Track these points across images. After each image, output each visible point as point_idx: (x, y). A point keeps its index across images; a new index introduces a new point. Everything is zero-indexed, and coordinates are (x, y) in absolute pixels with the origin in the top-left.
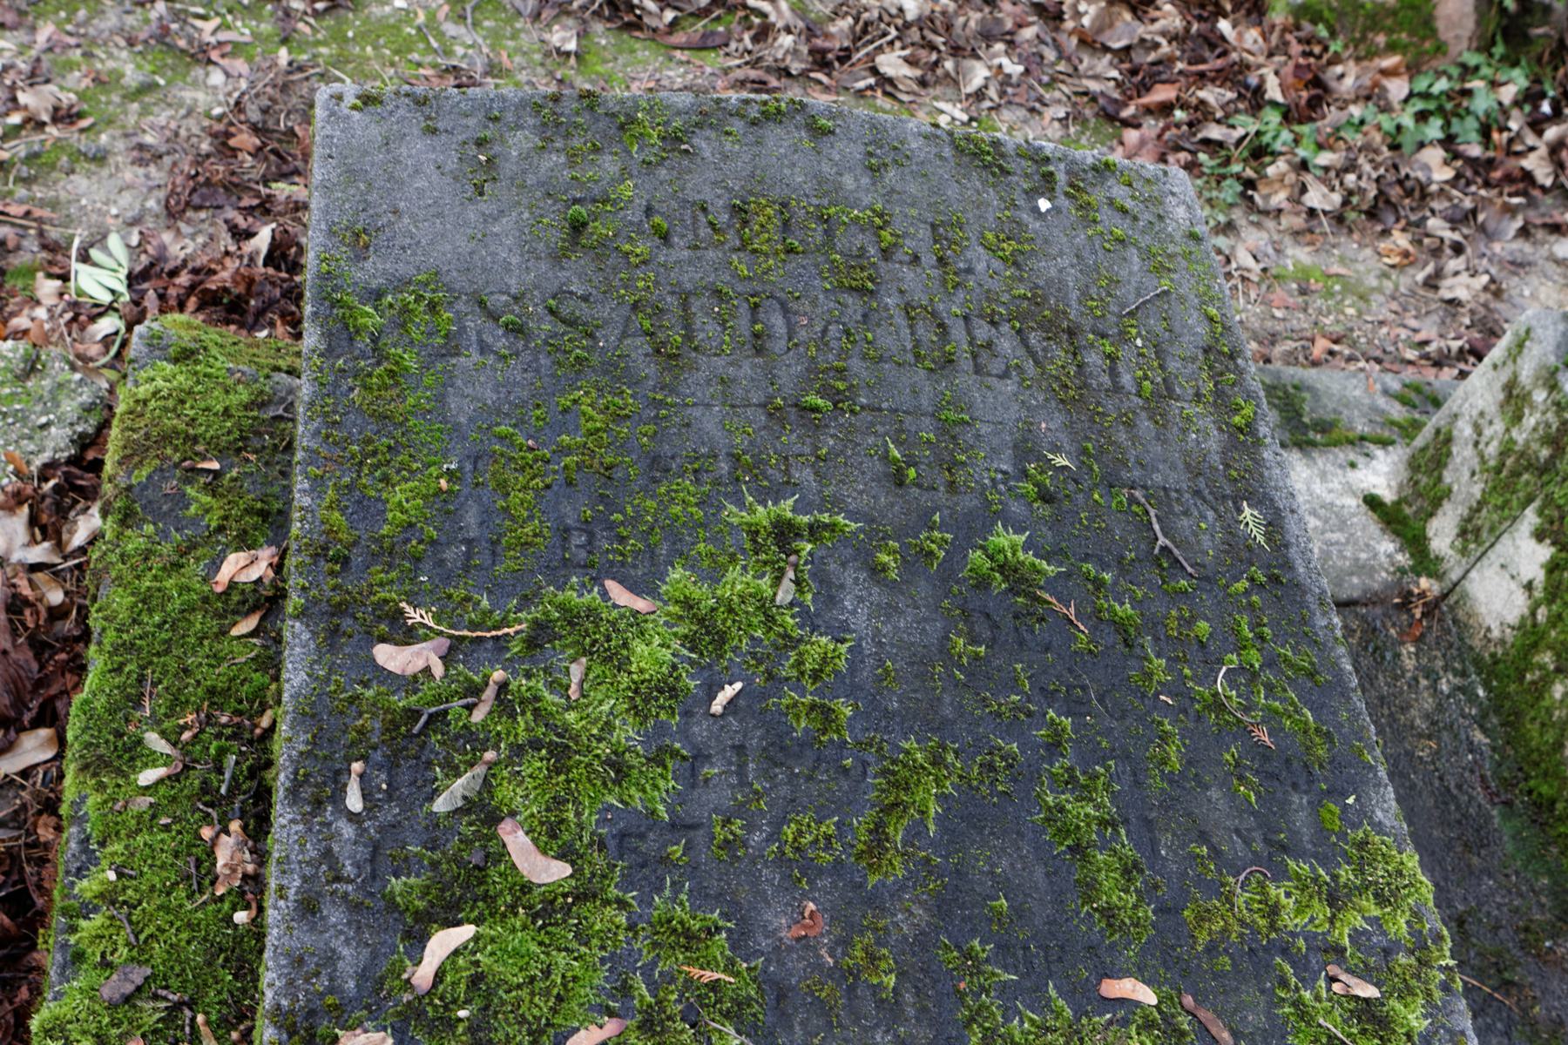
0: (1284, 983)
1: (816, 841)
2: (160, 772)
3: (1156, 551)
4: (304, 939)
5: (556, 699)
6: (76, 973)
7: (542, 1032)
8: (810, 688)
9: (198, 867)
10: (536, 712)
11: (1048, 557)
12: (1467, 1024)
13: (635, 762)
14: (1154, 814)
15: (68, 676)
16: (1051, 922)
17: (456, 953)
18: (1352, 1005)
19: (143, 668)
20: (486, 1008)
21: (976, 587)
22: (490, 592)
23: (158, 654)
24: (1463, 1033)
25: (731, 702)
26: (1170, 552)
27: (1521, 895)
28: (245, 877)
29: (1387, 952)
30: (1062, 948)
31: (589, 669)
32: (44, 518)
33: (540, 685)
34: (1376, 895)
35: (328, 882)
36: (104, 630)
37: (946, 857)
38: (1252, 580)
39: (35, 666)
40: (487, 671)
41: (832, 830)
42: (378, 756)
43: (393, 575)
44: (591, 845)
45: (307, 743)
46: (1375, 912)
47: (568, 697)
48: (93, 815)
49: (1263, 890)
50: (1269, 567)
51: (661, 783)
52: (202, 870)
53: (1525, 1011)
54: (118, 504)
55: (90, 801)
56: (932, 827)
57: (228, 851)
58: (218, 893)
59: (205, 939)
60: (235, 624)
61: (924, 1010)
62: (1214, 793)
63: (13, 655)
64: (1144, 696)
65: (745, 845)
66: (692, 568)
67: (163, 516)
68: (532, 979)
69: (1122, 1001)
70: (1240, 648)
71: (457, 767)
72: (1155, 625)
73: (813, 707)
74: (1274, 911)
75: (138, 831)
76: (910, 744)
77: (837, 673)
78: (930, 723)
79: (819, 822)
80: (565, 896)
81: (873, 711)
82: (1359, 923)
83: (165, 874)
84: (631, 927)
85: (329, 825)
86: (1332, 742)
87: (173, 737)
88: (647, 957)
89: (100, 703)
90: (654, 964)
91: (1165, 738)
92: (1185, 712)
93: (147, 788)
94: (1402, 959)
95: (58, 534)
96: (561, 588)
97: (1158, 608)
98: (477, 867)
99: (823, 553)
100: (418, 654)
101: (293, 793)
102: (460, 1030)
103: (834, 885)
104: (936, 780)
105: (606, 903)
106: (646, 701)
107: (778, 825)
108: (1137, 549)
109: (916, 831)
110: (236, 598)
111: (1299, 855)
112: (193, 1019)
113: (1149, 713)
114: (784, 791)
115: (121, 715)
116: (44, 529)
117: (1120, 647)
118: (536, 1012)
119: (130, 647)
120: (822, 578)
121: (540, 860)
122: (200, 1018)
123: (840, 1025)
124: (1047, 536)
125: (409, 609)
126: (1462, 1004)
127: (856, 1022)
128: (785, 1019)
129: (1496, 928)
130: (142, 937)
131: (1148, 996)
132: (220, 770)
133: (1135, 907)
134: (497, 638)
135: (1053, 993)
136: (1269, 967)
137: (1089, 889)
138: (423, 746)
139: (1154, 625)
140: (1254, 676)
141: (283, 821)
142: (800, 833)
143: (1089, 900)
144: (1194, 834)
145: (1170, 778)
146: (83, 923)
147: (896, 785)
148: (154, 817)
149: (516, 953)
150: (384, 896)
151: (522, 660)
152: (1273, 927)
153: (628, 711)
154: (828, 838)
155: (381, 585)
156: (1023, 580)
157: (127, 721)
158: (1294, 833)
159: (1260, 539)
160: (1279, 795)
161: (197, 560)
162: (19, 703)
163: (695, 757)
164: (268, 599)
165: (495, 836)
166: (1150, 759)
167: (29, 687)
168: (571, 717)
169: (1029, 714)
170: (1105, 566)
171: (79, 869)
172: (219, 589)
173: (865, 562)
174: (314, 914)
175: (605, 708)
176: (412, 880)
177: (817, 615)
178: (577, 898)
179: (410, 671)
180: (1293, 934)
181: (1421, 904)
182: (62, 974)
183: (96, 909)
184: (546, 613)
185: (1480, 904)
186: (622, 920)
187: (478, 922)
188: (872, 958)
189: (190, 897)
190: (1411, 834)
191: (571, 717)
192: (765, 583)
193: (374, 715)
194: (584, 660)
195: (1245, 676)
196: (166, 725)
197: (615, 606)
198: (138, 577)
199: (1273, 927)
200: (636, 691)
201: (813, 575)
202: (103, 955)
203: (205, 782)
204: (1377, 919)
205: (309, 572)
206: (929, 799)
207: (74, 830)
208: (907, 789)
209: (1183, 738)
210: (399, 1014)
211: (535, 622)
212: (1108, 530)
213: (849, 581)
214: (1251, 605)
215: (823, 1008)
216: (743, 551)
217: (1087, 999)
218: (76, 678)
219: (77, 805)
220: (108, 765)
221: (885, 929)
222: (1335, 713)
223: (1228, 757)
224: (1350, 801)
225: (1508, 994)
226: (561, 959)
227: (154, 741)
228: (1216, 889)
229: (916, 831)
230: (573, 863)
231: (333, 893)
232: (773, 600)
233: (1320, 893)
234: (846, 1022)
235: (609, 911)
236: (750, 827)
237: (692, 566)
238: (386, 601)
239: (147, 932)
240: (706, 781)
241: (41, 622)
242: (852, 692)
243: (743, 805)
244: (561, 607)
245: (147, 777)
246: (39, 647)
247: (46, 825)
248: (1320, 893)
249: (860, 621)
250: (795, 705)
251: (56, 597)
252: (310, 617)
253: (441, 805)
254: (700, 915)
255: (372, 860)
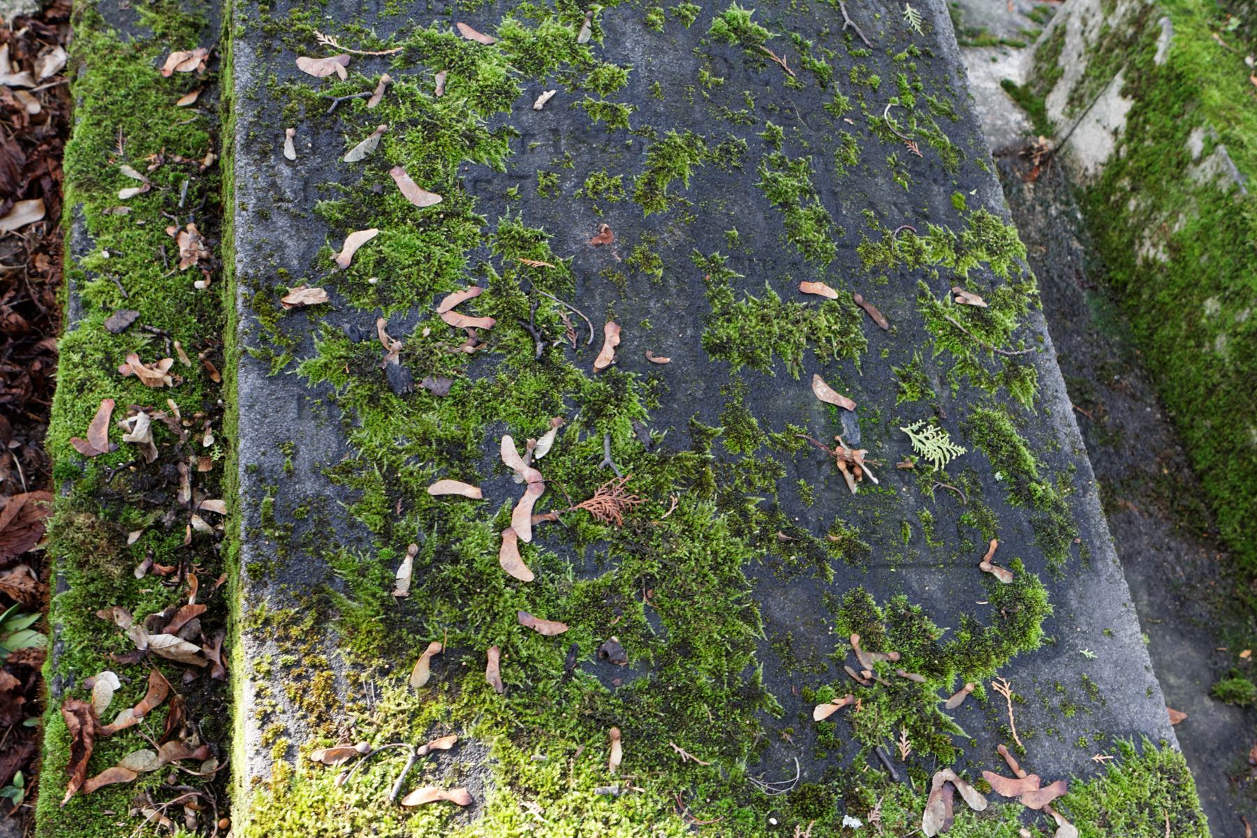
0: (923, 295)
1: (608, 188)
2: (134, 191)
3: (844, 28)
4: (260, 234)
5: (427, 96)
6: (87, 313)
7: (426, 294)
8: (602, 95)
9: (167, 252)
10: (413, 102)
11: (768, 26)
12: (1045, 329)
13: (483, 136)
14: (838, 189)
15: (49, 161)
16: (767, 246)
17: (365, 246)
18: (968, 311)
19: (116, 124)
20: (388, 279)
21: (717, 41)
22: (376, 28)
23: (126, 115)
24: (1041, 333)
25: (548, 102)
26: (854, 30)
27: (1099, 346)
28: (201, 260)
29: (993, 284)
30: (775, 262)
31: (449, 78)
32: (20, 54)
33: (415, 86)
34: (988, 249)
35: (275, 201)
36: (84, 98)
37: (697, 202)
38: (911, 52)
39: (23, 157)
40: (377, 76)
41: (619, 182)
42: (304, 127)
43: (307, 14)
44: (454, 185)
45: (254, 116)
46: (986, 259)
47: (435, 95)
48: (88, 217)
49: (911, 240)
50: (923, 46)
51: (502, 150)
52: (170, 255)
53: (1098, 419)
54: (87, 14)
55: (85, 208)
56: (687, 185)
57: (188, 242)
58: (183, 269)
59: (175, 297)
60: (180, 99)
61: (682, 290)
62: (880, 180)
63: (6, 147)
64: (833, 119)
65: (560, 188)
66: (519, 17)
67: (122, 25)
68: (418, 262)
69: (815, 296)
70: (900, 93)
71: (359, 135)
72: (842, 75)
73: (605, 107)
74: (919, 252)
75: (122, 228)
76: (673, 133)
77: (621, 87)
78: (686, 122)
79: (610, 177)
80: (438, 214)
81: (645, 109)
82: (975, 264)
83: (143, 255)
84: (484, 235)
85: (273, 167)
86: (962, 157)
87: (142, 169)
88: (495, 252)
89: (87, 144)
90: (500, 257)
91: (847, 144)
92: (862, 130)
93: (126, 201)
94: (1003, 287)
95: (31, 67)
96: (427, 27)
97: (844, 65)
98: (377, 194)
99: (610, 12)
100: (328, 64)
101: (247, 147)
102: (371, 291)
103: (621, 215)
104: (690, 155)
105: (466, 220)
106: (489, 99)
107: (582, 177)
108: (831, 27)
109: (676, 186)
110: (179, 81)
111: (936, 221)
112: (171, 345)
113: (837, 129)
114: (586, 157)
115: (101, 153)
116: (20, 62)
117: (817, 87)
118: (421, 281)
119: (105, 109)
120: (609, 26)
121: (421, 193)
122: (176, 344)
123: (626, 297)
124: (767, 14)
125: (320, 36)
126: (1042, 317)
127: (637, 295)
128: (589, 291)
129: (1081, 368)
130: (131, 294)
131: (832, 294)
132: (177, 192)
133: (824, 241)
134: (383, 57)
135: (768, 287)
136: (913, 284)
137: (794, 228)
138: (335, 122)
139: (842, 75)
140: (910, 112)
141: (241, 164)
142: (598, 183)
143: (793, 236)
144: (865, 204)
145: (850, 169)
146: (87, 283)
147: (663, 157)
148: (132, 220)
149: (407, 246)
150: (314, 211)
151: (401, 71)
152: (917, 261)
153: (476, 105)
154: (616, 187)
155: (299, 20)
156: (750, 39)
157: (108, 158)
158: (933, 208)
159: (918, 28)
160: (924, 185)
161: (149, 55)
162: (13, 182)
163: (524, 135)
164: (203, 83)
165: (390, 177)
166: (837, 156)
167: (19, 171)
168: (438, 107)
169: (754, 122)
170: (809, 37)
171: (82, 250)
172: (167, 75)
173: (640, 19)
174: (266, 220)
175: (461, 102)
176: (333, 202)
177: (607, 51)
178: (446, 215)
179: (322, 75)
180: (930, 267)
181: (1017, 256)
182: (76, 314)
183: (96, 275)
184: (417, 42)
185: (1071, 352)
186: (478, 230)
187: (381, 227)
188: (647, 258)
189: (163, 270)
190: (1013, 216)
191: (438, 107)
192: (570, 30)
193: (300, 102)
194: (445, 72)
195: (903, 111)
196: (135, 161)
197: (465, 40)
198: (106, 64)
199: (917, 261)
200: (482, 92)
201: (603, 25)
202: (104, 302)
203: (167, 198)
204: (988, 263)
205: (247, 10)
206: (685, 166)
207: (75, 226)
208: (670, 159)
209: (859, 145)
210: (329, 280)
211: (410, 47)
212: (810, 13)
213: (629, 31)
214: (909, 68)
215: (617, 287)
216: (554, 8)
217: (791, 292)
218: (55, 163)
219: (76, 210)
220: (96, 184)
221: (656, 242)
222: (965, 140)
223: (890, 159)
224: (973, 193)
225: (1086, 409)
226: (437, 251)
227: (127, 170)
228: (879, 236)
229: (676, 186)
230: (443, 195)
231: (279, 208)
232: (576, 39)
233: (949, 244)
234: (630, 295)
235: (468, 225)
236: (564, 178)
237: (518, 15)
238: (303, 30)
239: (134, 291)
240: (533, 149)
241: (26, 124)
242: (631, 100)
243: (557, 165)
244: (427, 38)
245: (125, 193)
246: (26, 145)
247: (42, 261)
248: (949, 244)
249: (637, 55)
250: (592, 105)
251: (34, 108)
252: (250, 38)
253: (350, 158)
254: (530, 229)
255: (304, 190)
